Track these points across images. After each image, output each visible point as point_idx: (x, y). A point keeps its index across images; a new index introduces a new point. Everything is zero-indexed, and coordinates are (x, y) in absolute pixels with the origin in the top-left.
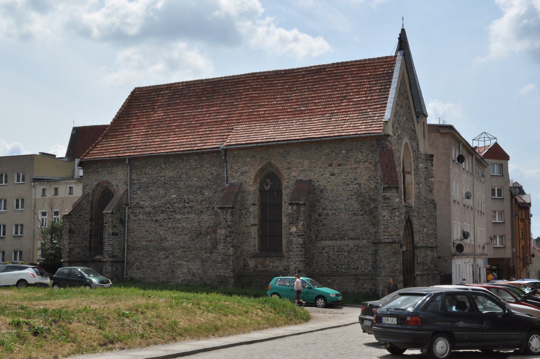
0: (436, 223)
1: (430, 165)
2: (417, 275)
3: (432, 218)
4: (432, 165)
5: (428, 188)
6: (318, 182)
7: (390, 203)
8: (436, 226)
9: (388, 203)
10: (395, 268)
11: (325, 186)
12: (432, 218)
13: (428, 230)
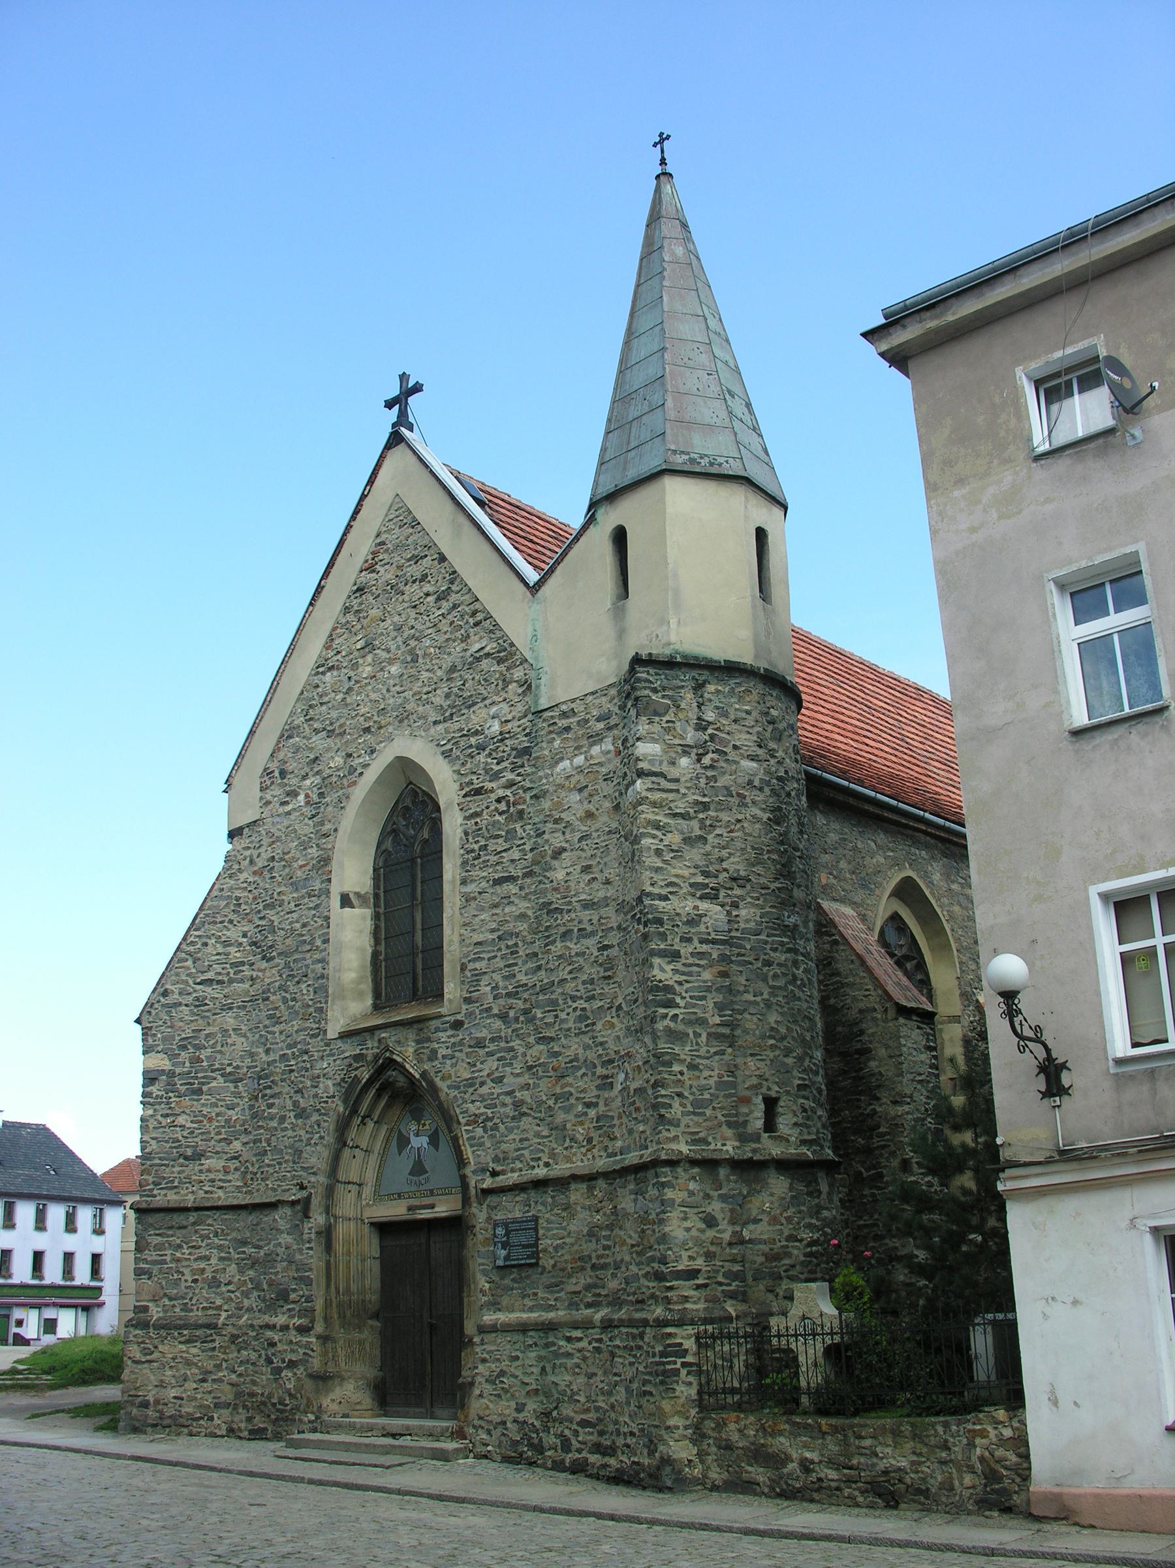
2: (482, 1330)
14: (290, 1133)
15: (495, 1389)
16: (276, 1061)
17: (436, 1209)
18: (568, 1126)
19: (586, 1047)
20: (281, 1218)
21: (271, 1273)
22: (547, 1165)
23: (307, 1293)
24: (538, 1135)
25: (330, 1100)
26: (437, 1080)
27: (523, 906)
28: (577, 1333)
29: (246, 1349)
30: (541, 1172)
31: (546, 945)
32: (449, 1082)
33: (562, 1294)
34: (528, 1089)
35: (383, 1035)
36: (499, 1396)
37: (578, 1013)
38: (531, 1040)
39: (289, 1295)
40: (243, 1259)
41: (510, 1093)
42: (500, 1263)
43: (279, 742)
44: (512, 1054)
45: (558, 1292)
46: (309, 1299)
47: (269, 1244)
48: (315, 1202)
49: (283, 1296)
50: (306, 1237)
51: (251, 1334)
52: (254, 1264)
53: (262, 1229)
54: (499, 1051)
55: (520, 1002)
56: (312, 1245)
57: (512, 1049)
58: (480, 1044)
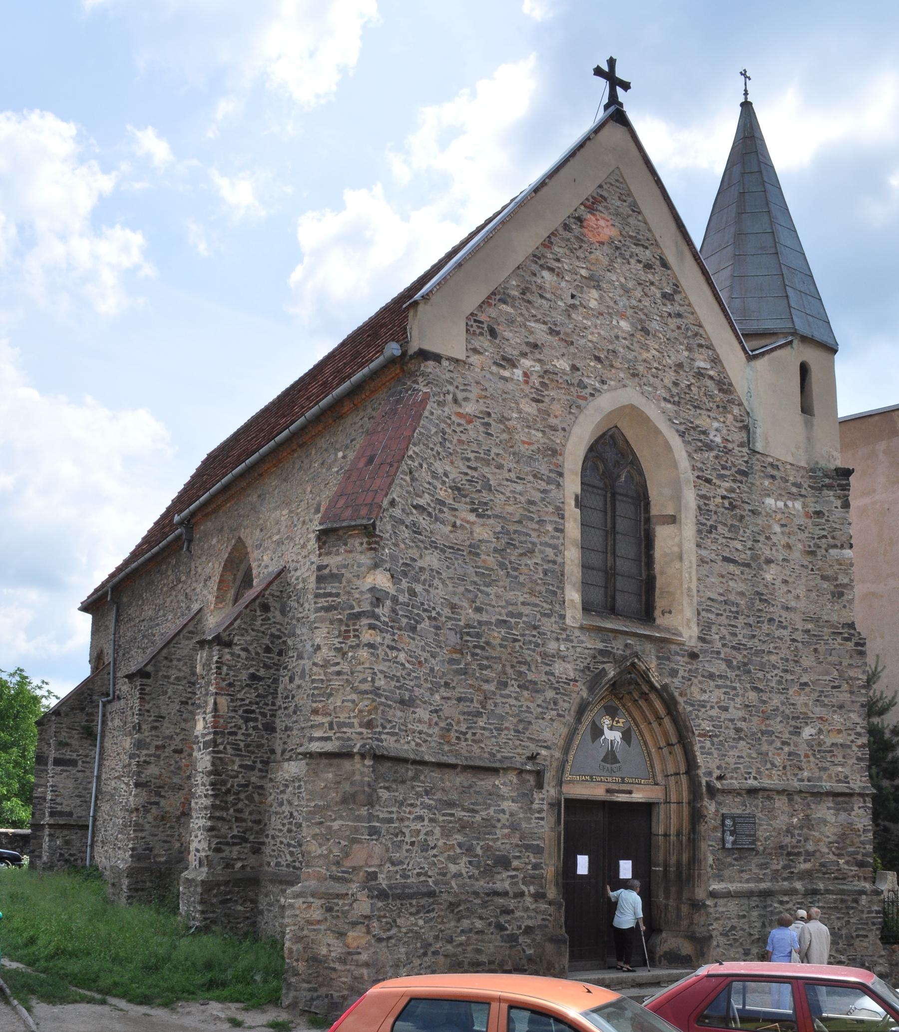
1: (839, 503)
2: (713, 895)
3: (845, 687)
4: (846, 505)
5: (825, 585)
12: (845, 687)
13: (820, 731)
14: (512, 702)
15: (728, 940)
16: (491, 623)
17: (633, 795)
18: (770, 754)
19: (783, 703)
20: (505, 784)
21: (488, 839)
22: (755, 778)
23: (534, 861)
24: (749, 756)
25: (572, 683)
26: (676, 694)
27: (740, 587)
28: (786, 899)
29: (468, 917)
30: (752, 783)
31: (758, 622)
32: (685, 699)
33: (768, 871)
34: (745, 721)
35: (629, 641)
36: (731, 945)
37: (778, 678)
38: (748, 686)
39: (510, 863)
40: (450, 822)
41: (732, 720)
42: (728, 846)
43: (489, 297)
44: (734, 692)
46: (536, 867)
47: (488, 809)
48: (548, 776)
49: (504, 862)
50: (535, 806)
51: (475, 901)
52: (463, 827)
53: (477, 793)
54: (727, 687)
55: (741, 656)
56: (544, 815)
57: (735, 688)
58: (711, 676)
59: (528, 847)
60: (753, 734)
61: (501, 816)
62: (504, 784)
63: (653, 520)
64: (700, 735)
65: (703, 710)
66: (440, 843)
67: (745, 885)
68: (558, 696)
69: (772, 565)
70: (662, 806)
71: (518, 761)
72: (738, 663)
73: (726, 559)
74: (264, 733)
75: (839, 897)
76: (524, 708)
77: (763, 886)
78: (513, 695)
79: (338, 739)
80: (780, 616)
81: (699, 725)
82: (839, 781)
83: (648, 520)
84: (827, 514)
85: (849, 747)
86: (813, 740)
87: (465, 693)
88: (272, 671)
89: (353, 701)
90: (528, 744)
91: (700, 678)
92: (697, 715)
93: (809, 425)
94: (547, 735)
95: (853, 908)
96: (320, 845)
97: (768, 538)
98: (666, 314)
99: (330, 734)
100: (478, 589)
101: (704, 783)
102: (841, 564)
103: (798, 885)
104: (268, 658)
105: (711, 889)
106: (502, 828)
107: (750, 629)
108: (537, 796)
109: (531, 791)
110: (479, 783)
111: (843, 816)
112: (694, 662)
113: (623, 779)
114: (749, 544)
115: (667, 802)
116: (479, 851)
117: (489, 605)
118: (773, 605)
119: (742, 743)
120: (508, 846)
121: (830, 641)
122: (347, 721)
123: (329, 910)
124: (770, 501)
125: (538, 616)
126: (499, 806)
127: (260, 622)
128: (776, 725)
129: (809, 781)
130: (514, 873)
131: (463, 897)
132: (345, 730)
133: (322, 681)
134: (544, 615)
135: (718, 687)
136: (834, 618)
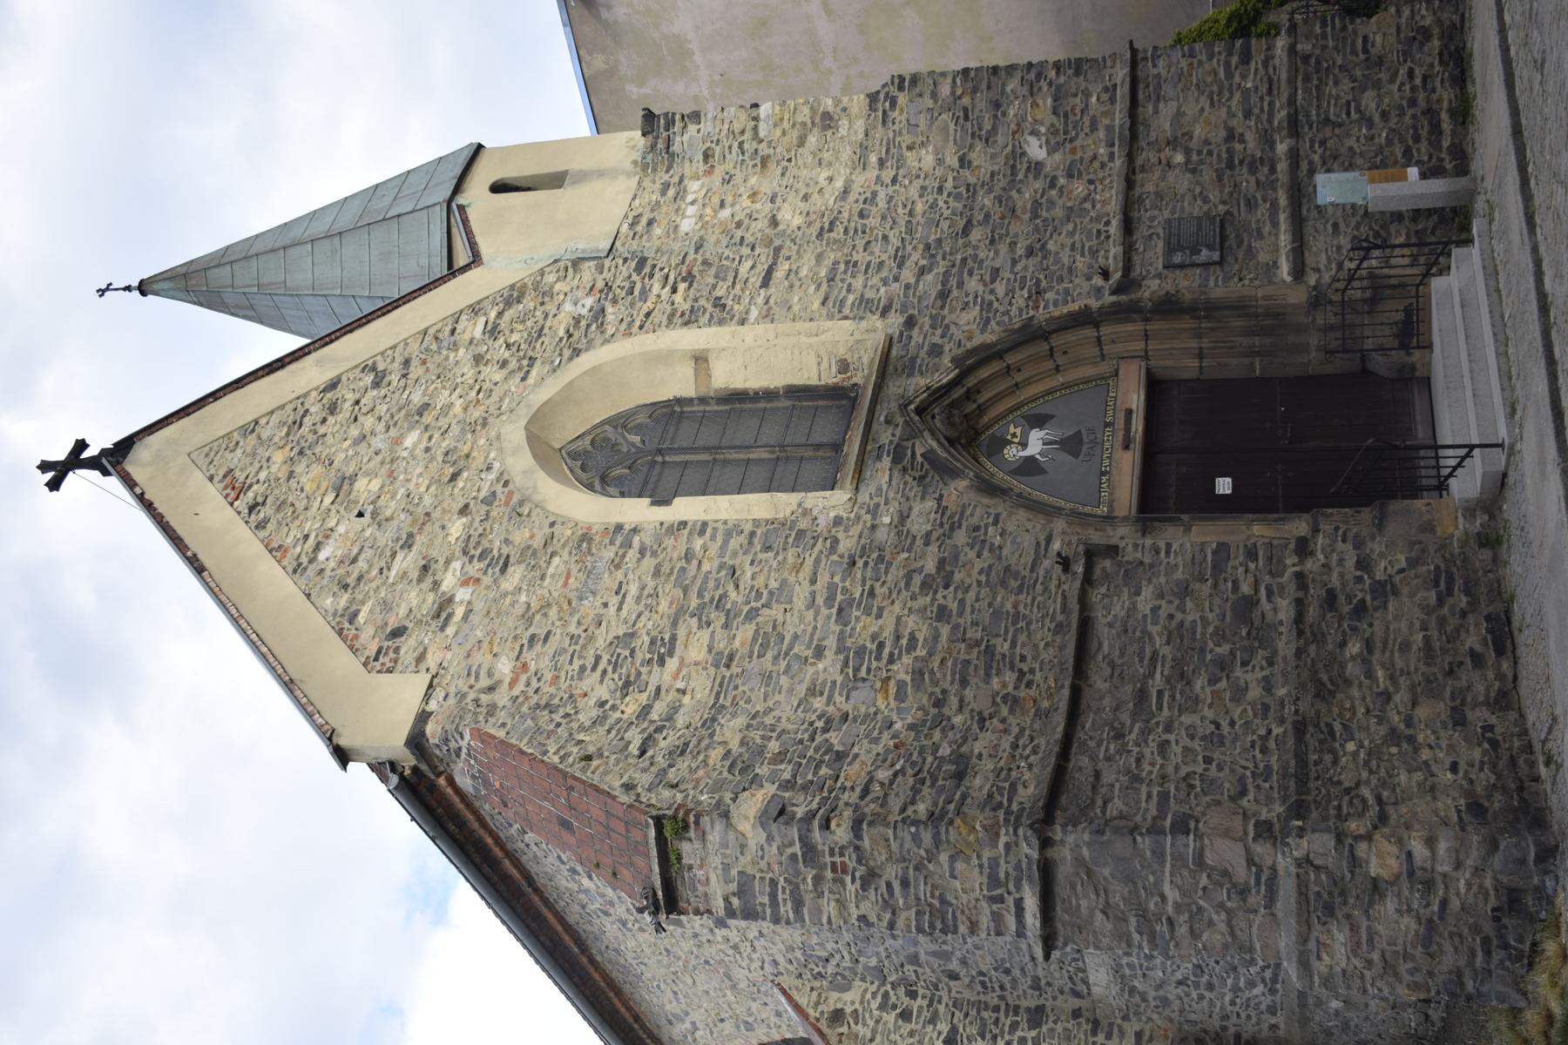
0: (995, 70)
3: (966, 101)
5: (812, 140)
6: (775, 963)
7: (774, 883)
8: (1011, 69)
9: (773, 896)
10: (1241, 873)
11: (791, 949)
12: (966, 101)
13: (1034, 133)
14: (971, 595)
16: (842, 632)
17: (1134, 407)
18: (1069, 204)
19: (990, 191)
20: (1110, 610)
21: (1203, 634)
22: (1108, 223)
23: (1241, 558)
24: (1071, 234)
26: (969, 345)
28: (1304, 166)
29: (1342, 666)
30: (1114, 228)
31: (864, 232)
33: (1259, 196)
34: (1015, 243)
35: (882, 418)
37: (951, 200)
39: (1245, 597)
40: (1173, 698)
41: (1014, 262)
42: (1216, 256)
44: (969, 261)
45: (1256, 199)
46: (1252, 554)
48: (1096, 537)
49: (1246, 607)
51: (1313, 654)
52: (1182, 675)
53: (1122, 653)
54: (961, 273)
55: (914, 254)
57: (964, 260)
59: (1218, 568)
60: (1037, 229)
61: (1163, 613)
62: (1108, 609)
63: (703, 391)
64: (1036, 308)
65: (996, 305)
66: (1209, 714)
67: (1283, 227)
68: (964, 524)
69: (779, 217)
70: (1152, 363)
71: (1073, 587)
72: (924, 258)
73: (766, 283)
74: (1045, 1028)
75: (1299, 84)
76: (983, 578)
77: (1283, 200)
78: (960, 595)
79: (1018, 887)
80: (857, 201)
81: (1020, 310)
82: (1113, 101)
83: (703, 400)
84: (708, 144)
85: (1059, 87)
86: (1047, 142)
87: (953, 674)
88: (942, 1008)
89: (952, 859)
90: (1042, 572)
91: (946, 312)
92: (1003, 314)
93: (583, 177)
94: (1027, 541)
95: (1318, 62)
96: (1211, 924)
97: (739, 225)
98: (403, 381)
99: (1010, 901)
100: (786, 654)
101: (1113, 298)
102: (782, 119)
103: (1282, 148)
104: (918, 1016)
105: (1289, 279)
106: (1184, 612)
107: (873, 244)
108: (1131, 555)
109: (1120, 565)
110: (1106, 648)
111: (1167, 90)
112: (921, 321)
113: (1107, 425)
114: (745, 251)
115: (1146, 357)
116: (1224, 649)
117: (812, 635)
118: (840, 212)
119: (1051, 246)
120: (1217, 601)
121: (896, 127)
122: (986, 871)
123: (1329, 909)
124: (686, 225)
125: (835, 558)
126: (1145, 616)
127: (860, 1027)
128: (1024, 199)
129: (1113, 145)
130: (1263, 592)
131: (1305, 674)
132: (1002, 875)
133: (919, 913)
134: (833, 549)
135: (960, 285)
136: (860, 125)
